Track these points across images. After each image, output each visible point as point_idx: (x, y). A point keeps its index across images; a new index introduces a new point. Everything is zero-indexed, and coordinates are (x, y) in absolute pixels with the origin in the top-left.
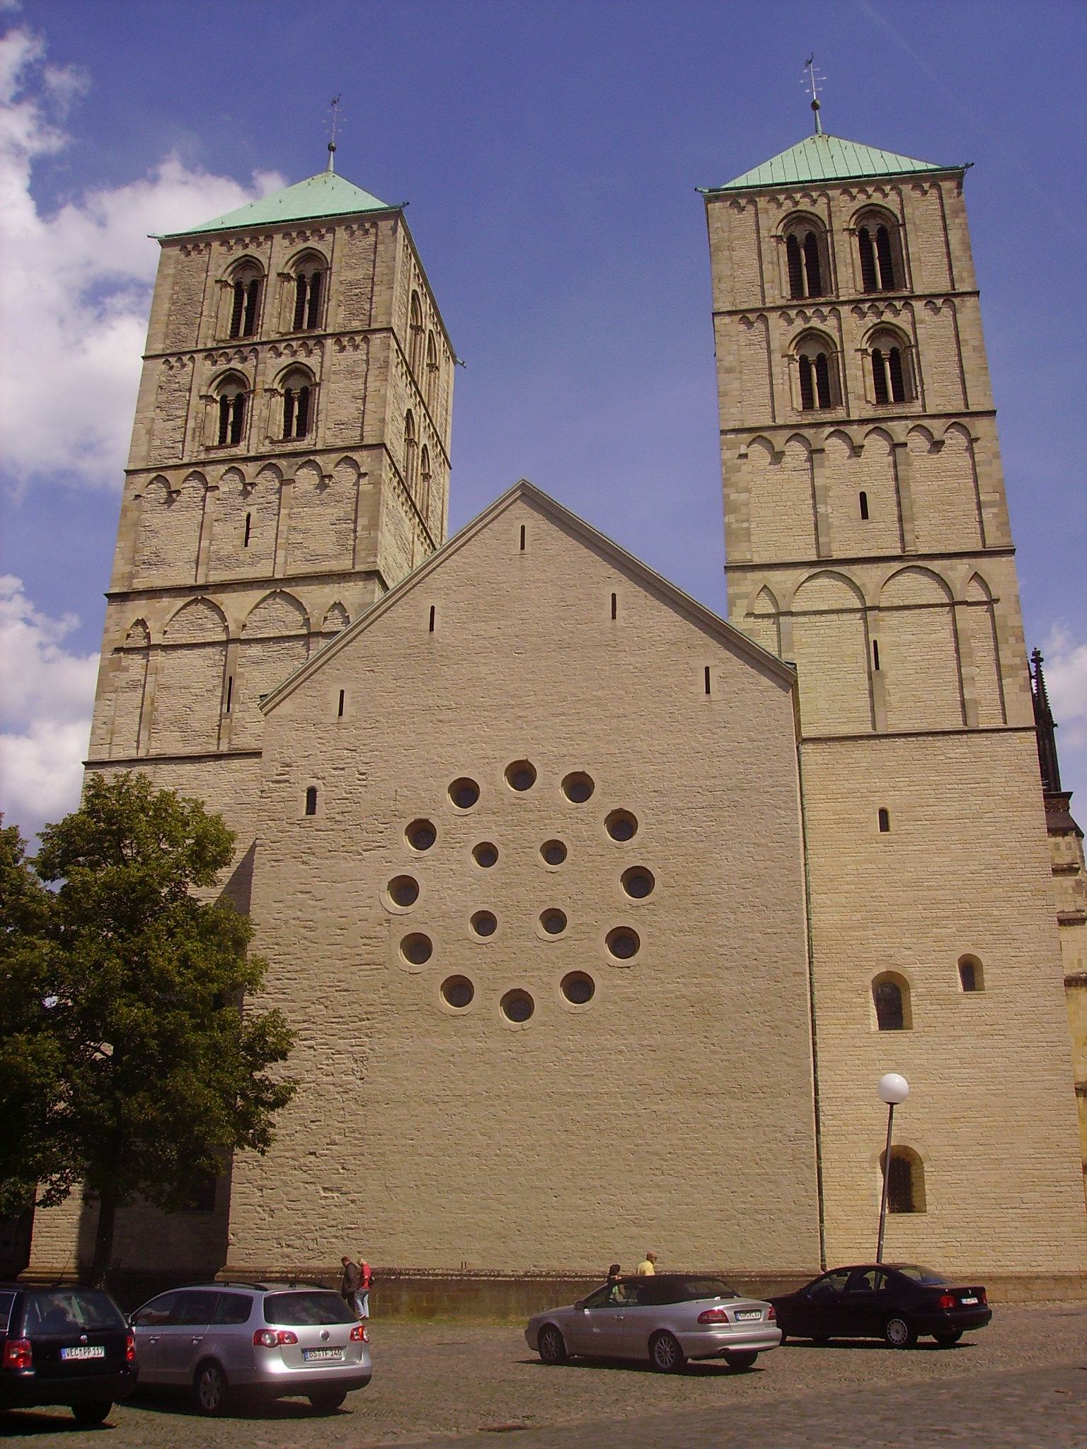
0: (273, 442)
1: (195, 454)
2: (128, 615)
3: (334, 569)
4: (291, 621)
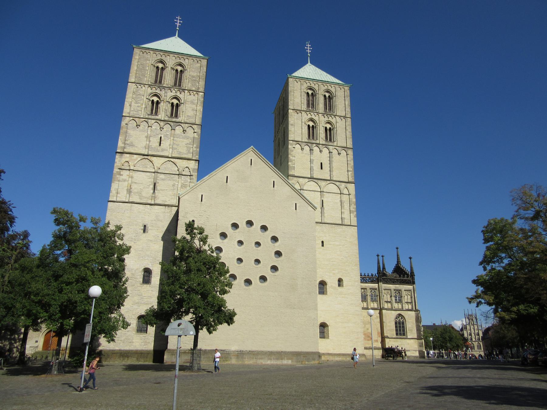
0: (168, 117)
1: (144, 115)
3: (186, 157)
4: (174, 170)
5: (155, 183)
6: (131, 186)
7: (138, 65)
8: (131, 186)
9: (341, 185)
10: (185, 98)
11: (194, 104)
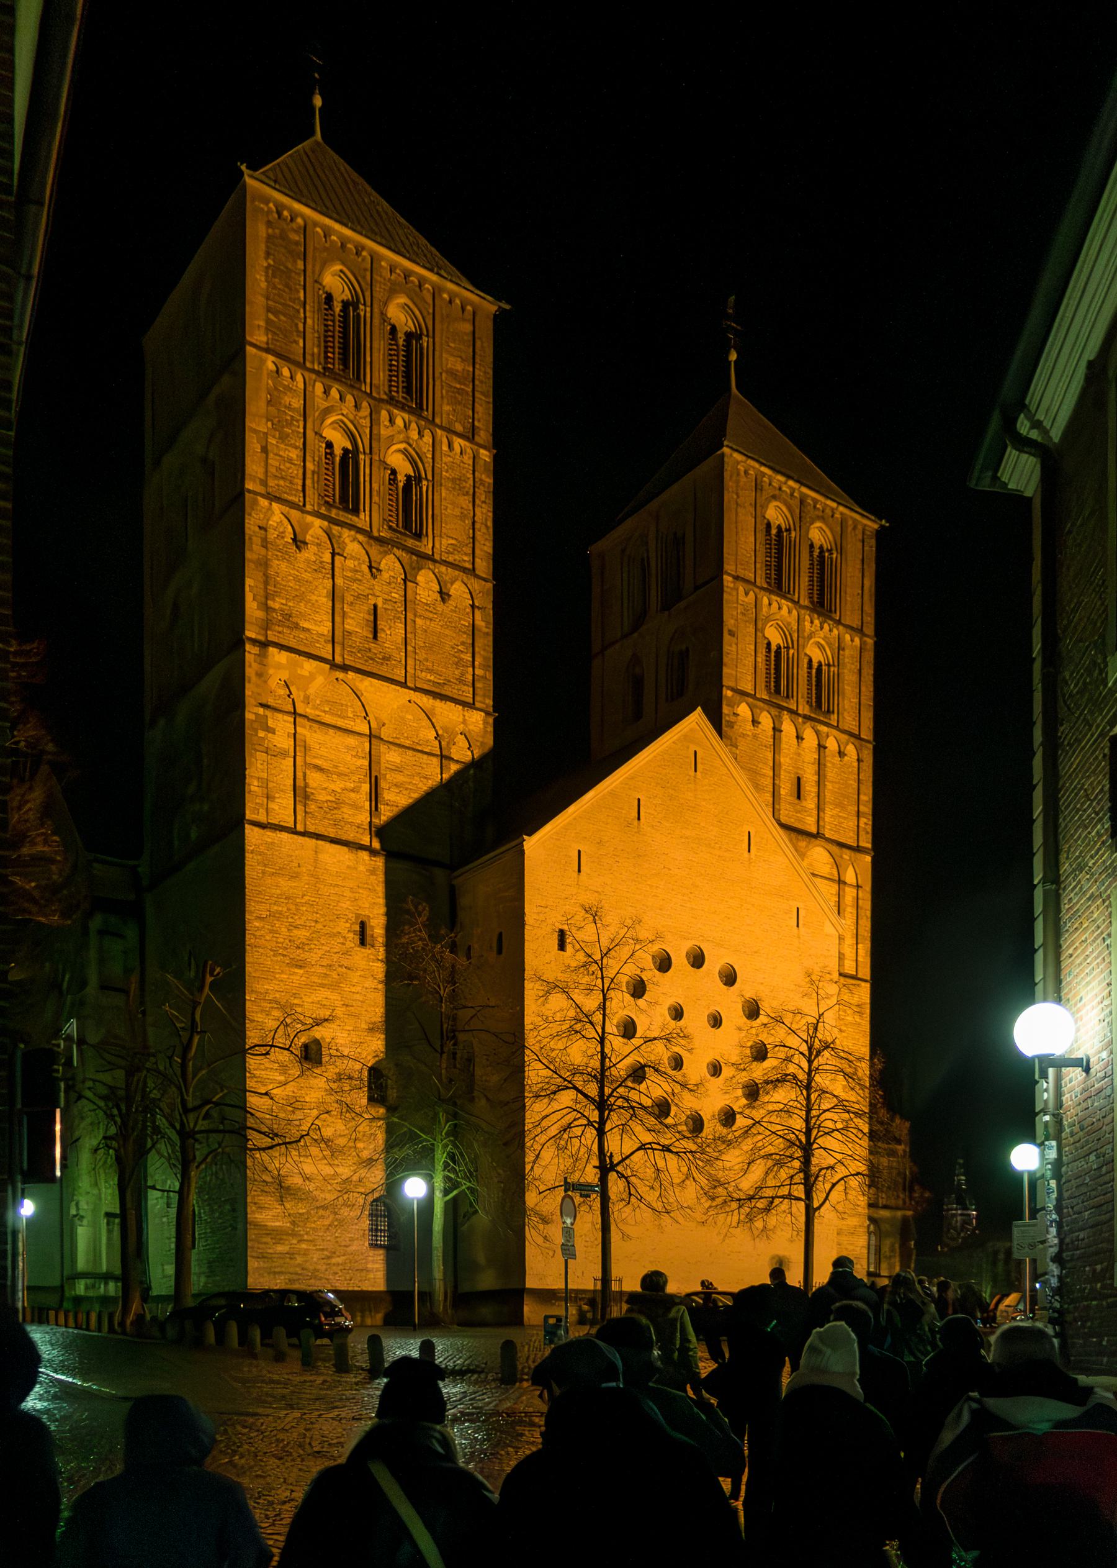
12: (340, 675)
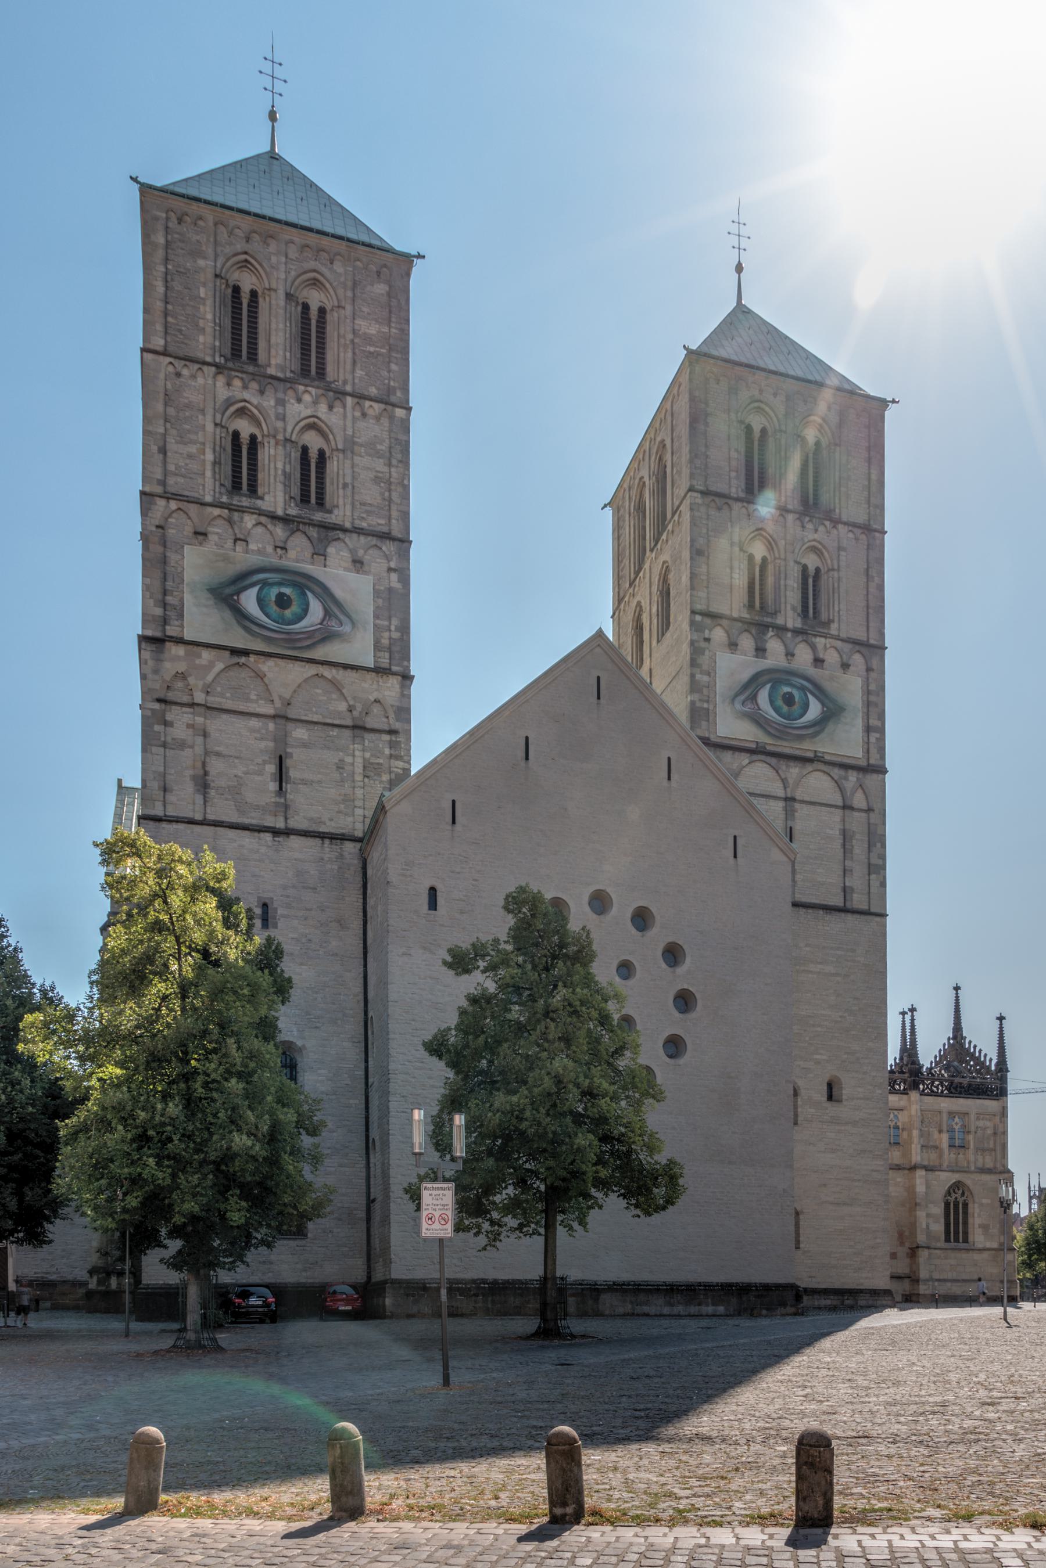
2: (167, 665)
5: (281, 757)
6: (204, 764)
7: (166, 274)
8: (204, 764)
9: (846, 778)
10: (349, 432)
11: (378, 455)
12: (243, 660)
